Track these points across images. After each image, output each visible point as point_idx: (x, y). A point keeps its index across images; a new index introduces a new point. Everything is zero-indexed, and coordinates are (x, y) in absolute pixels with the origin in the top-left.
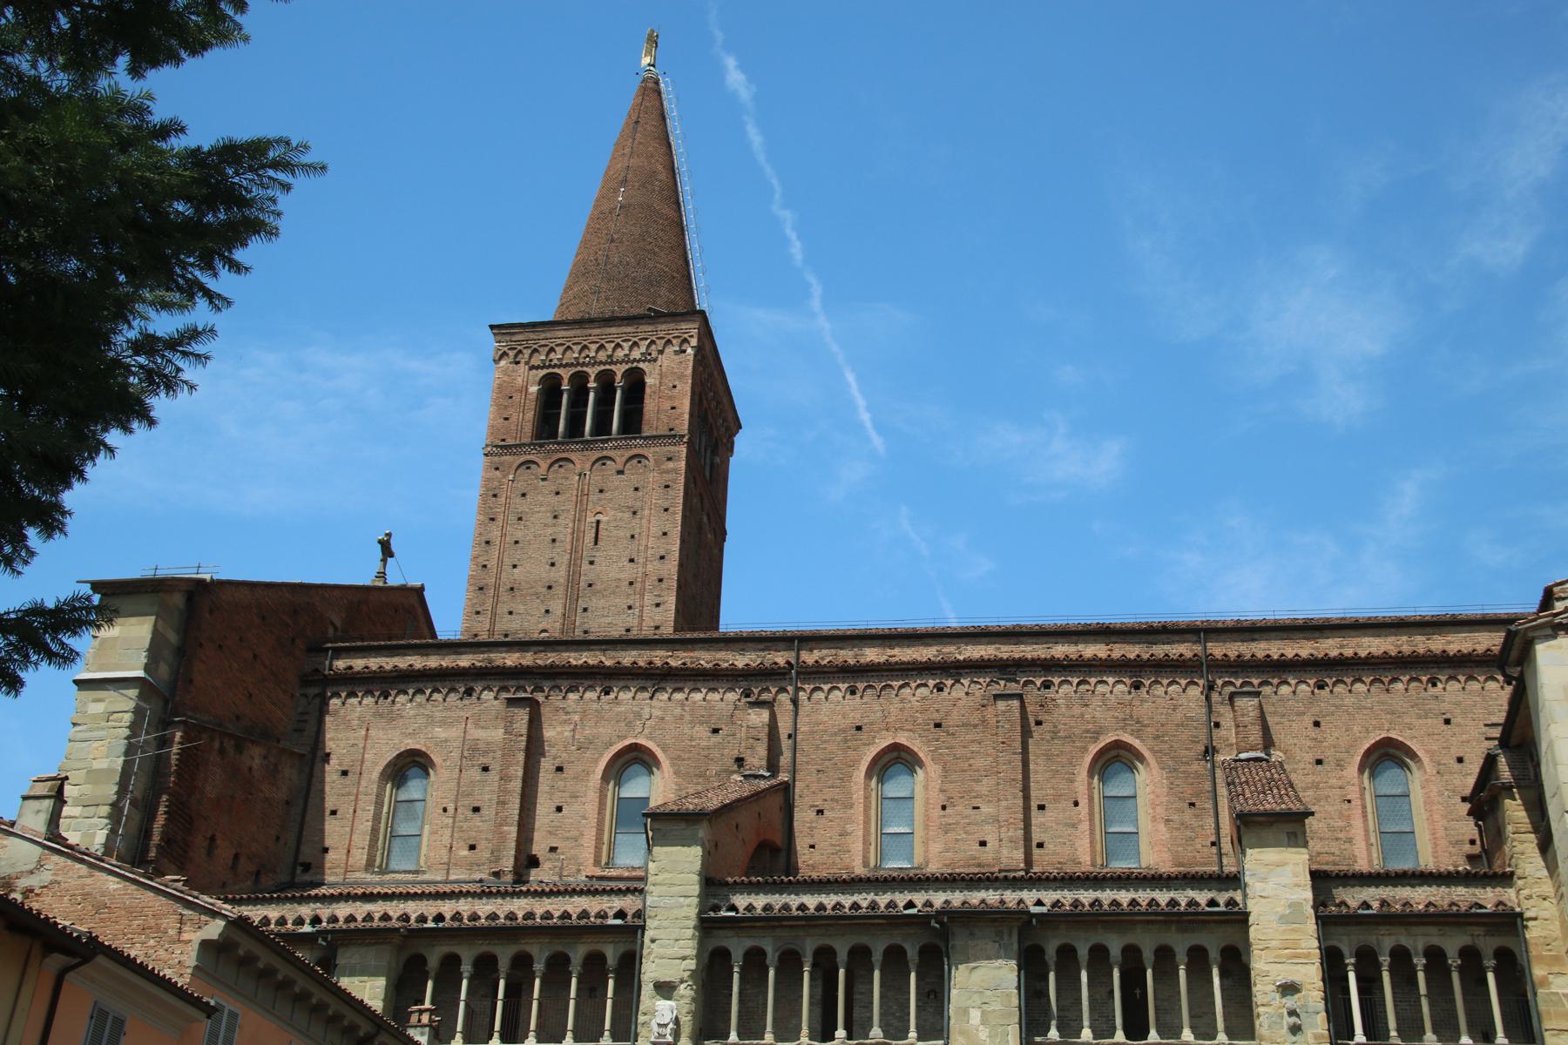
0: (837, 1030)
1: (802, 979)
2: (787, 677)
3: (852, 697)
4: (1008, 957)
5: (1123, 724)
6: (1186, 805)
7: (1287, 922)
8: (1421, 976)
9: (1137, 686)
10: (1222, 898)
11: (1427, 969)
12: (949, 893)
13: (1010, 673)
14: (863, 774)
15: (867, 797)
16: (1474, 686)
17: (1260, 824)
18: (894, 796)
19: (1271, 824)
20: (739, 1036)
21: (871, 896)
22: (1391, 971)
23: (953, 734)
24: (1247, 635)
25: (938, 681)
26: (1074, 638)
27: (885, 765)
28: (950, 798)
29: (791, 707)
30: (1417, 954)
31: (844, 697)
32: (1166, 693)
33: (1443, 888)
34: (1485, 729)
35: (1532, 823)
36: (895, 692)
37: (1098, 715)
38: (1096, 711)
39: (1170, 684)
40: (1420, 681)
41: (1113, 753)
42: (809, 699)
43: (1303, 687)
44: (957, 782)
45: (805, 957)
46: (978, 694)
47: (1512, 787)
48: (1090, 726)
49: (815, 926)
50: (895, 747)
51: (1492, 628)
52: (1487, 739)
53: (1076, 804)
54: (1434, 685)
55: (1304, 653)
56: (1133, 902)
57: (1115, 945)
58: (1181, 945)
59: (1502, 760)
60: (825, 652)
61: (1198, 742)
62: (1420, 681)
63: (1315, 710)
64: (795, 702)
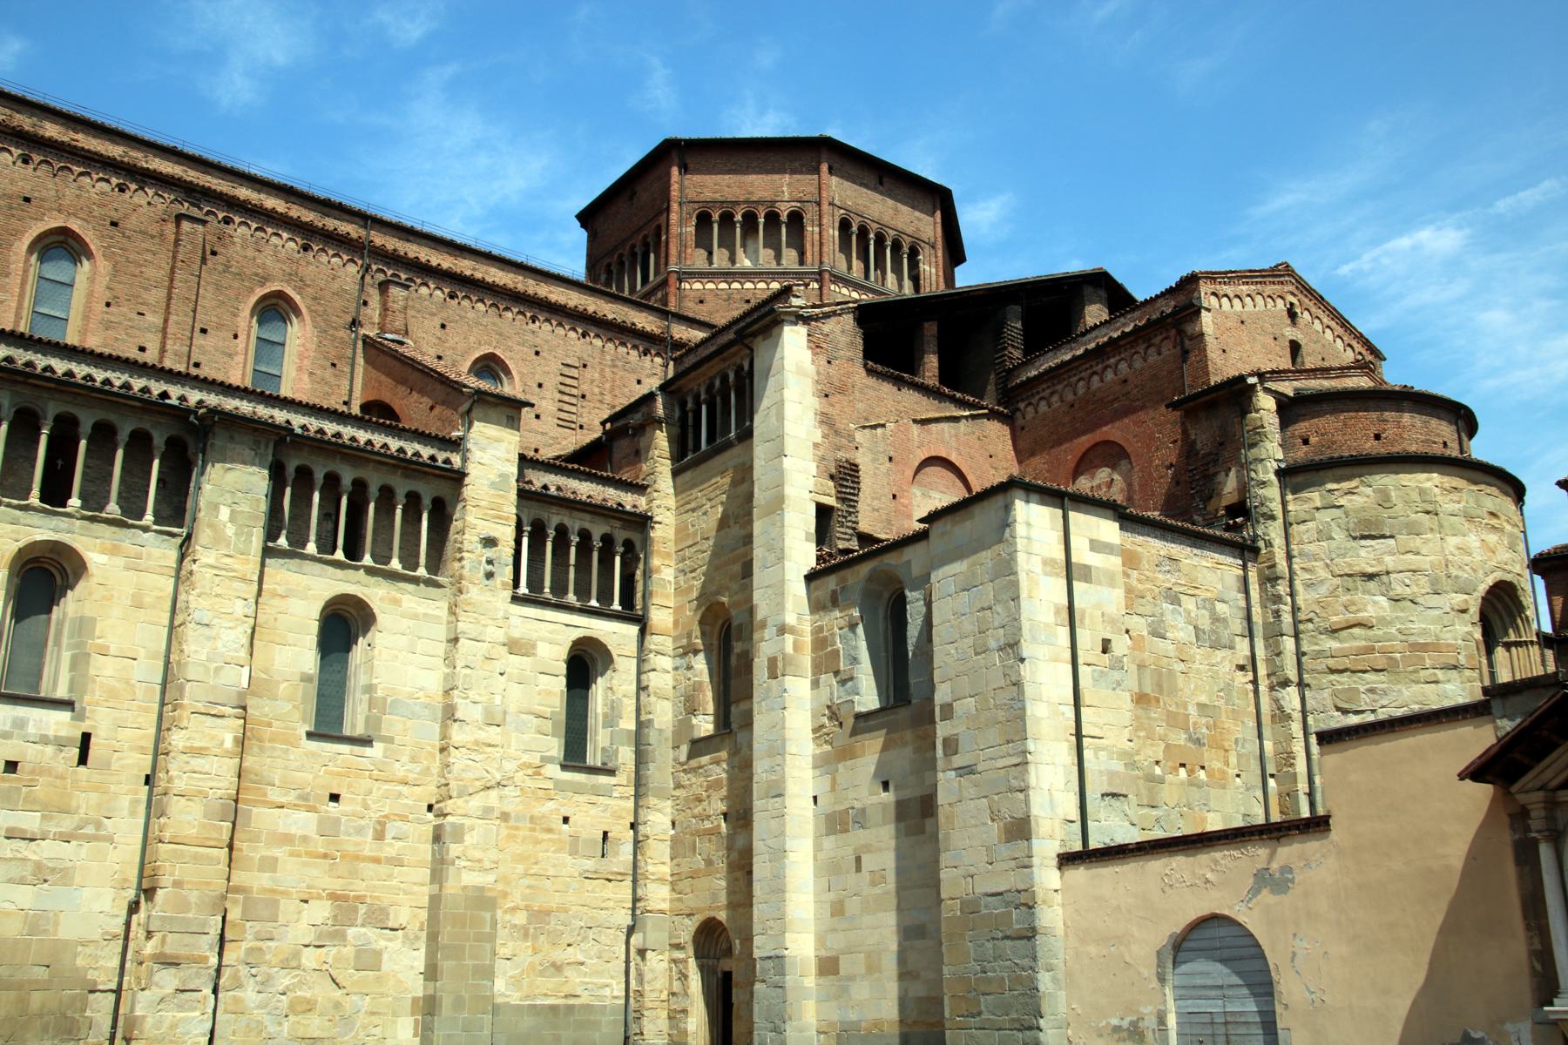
0: (70, 498)
1: (37, 442)
3: (24, 166)
4: (261, 465)
5: (290, 277)
7: (496, 489)
8: (573, 550)
9: (306, 248)
11: (578, 546)
12: (205, 393)
13: (194, 198)
14: (25, 248)
15: (26, 271)
16: (560, 331)
17: (488, 403)
18: (52, 278)
19: (496, 405)
21: (125, 377)
23: (129, 237)
24: (404, 235)
25: (121, 181)
26: (259, 186)
27: (47, 245)
28: (115, 297)
30: (573, 533)
31: (14, 163)
32: (329, 262)
33: (600, 487)
34: (561, 367)
35: (671, 452)
36: (73, 177)
37: (268, 262)
38: (267, 260)
39: (334, 255)
41: (274, 301)
43: (438, 292)
44: (125, 283)
45: (45, 419)
48: (260, 271)
49: (61, 391)
50: (64, 232)
51: (582, 291)
52: (562, 375)
53: (236, 337)
54: (534, 322)
56: (369, 442)
57: (347, 477)
58: (402, 487)
59: (660, 400)
61: (348, 313)
63: (444, 315)
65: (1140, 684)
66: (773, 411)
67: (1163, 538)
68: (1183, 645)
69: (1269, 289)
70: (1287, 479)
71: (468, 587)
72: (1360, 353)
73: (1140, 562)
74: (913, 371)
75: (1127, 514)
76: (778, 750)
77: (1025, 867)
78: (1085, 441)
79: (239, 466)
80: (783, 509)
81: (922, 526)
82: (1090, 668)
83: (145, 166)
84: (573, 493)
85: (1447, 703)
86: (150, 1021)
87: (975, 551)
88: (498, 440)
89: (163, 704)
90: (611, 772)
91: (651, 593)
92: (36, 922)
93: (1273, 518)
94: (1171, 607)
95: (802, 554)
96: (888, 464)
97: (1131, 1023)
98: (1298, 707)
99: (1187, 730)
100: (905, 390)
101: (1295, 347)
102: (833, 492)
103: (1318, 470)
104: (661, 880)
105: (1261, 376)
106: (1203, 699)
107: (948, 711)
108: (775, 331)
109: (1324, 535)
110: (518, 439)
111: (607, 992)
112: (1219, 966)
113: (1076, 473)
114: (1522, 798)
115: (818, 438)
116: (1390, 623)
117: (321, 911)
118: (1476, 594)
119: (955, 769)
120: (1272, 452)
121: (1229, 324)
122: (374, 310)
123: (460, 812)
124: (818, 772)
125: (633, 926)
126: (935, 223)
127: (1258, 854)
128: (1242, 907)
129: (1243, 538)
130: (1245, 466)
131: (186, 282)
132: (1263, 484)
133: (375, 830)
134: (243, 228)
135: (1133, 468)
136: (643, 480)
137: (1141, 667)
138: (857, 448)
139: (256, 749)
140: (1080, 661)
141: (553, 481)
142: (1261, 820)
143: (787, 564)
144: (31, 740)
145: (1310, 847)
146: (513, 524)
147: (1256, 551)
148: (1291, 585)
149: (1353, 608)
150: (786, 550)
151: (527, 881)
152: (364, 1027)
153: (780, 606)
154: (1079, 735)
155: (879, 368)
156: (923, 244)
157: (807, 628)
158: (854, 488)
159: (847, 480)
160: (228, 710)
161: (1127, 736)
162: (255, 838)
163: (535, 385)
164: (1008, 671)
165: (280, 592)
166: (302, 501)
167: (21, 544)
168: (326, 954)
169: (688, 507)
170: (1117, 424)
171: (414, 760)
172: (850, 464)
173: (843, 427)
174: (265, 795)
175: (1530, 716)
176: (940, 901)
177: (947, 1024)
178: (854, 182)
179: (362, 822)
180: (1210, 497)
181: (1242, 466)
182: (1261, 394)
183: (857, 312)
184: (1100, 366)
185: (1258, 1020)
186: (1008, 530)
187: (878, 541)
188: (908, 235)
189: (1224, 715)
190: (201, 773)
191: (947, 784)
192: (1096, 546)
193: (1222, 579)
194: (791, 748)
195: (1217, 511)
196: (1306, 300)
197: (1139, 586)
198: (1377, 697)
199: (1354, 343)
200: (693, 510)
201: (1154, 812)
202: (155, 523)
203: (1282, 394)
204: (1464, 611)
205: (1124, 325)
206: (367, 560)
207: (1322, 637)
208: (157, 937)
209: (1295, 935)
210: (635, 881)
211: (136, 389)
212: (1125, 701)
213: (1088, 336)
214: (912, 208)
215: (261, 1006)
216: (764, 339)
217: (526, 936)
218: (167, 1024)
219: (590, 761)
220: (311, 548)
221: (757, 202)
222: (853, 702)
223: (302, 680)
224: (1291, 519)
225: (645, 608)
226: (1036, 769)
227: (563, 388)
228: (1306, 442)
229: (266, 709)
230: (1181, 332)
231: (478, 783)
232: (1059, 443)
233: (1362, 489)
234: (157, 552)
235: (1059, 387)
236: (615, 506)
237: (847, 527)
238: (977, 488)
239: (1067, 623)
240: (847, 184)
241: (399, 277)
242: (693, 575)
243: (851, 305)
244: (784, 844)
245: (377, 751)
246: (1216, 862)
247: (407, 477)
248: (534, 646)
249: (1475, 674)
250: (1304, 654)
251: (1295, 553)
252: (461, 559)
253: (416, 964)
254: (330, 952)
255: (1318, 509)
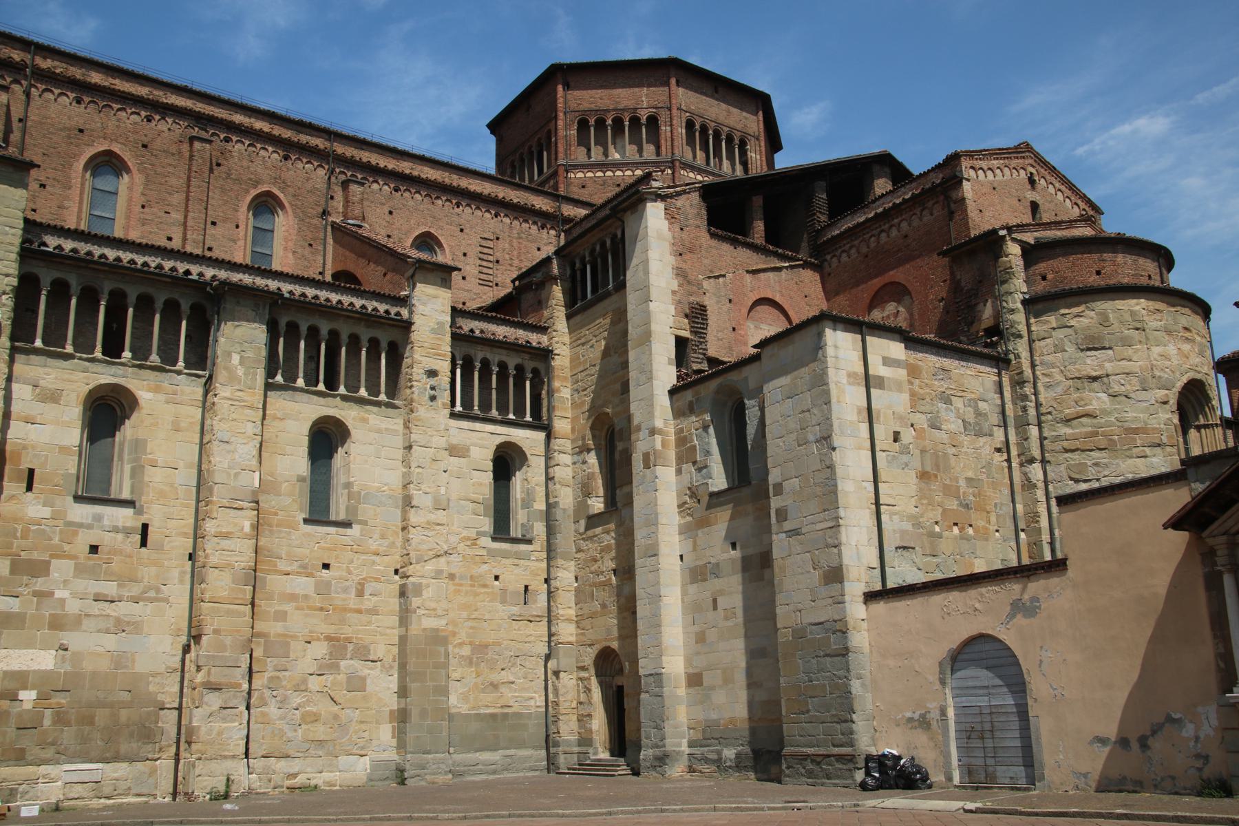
0: (123, 351)
1: (98, 311)
2: (22, 72)
3: (78, 105)
5: (275, 180)
6: (307, 245)
8: (494, 377)
9: (286, 158)
10: (393, 310)
11: (498, 374)
12: (217, 270)
13: (202, 124)
14: (81, 166)
15: (83, 185)
16: (478, 213)
18: (102, 188)
19: (433, 270)
20: (44, 342)
21: (158, 260)
22: (479, 372)
23: (155, 156)
25: (148, 114)
26: (250, 113)
29: (24, 98)
30: (494, 365)
31: (71, 104)
34: (480, 240)
36: (113, 112)
38: (257, 167)
39: (307, 163)
40: (452, 203)
41: (264, 199)
42: (40, 96)
43: (386, 187)
45: (103, 294)
46: (178, 132)
47: (557, 279)
48: (253, 177)
50: (109, 153)
52: (481, 246)
53: (237, 227)
54: (458, 207)
55: (390, 167)
56: (339, 302)
58: (365, 335)
59: (555, 262)
60: (57, 63)
62: (452, 203)
64: (28, 95)
65: (922, 464)
66: (641, 267)
67: (937, 354)
68: (953, 435)
69: (1014, 163)
70: (1031, 307)
71: (417, 408)
72: (1084, 210)
73: (921, 373)
74: (745, 235)
75: (910, 337)
76: (653, 522)
77: (839, 603)
78: (877, 283)
79: (245, 323)
80: (650, 342)
81: (756, 350)
82: (884, 454)
83: (165, 101)
84: (493, 334)
85: (1154, 472)
86: (203, 729)
87: (796, 369)
88: (436, 297)
89: (198, 501)
90: (529, 542)
91: (554, 407)
92: (119, 660)
93: (1020, 336)
94: (945, 406)
95: (665, 374)
96: (728, 305)
97: (921, 715)
98: (1042, 478)
99: (958, 498)
100: (739, 248)
101: (1034, 207)
102: (688, 327)
103: (1054, 299)
104: (569, 620)
105: (1009, 229)
106: (970, 474)
107: (779, 488)
108: (640, 207)
109: (1059, 349)
110: (450, 295)
111: (532, 703)
112: (985, 672)
113: (871, 307)
114: (1210, 541)
115: (676, 288)
116: (1110, 413)
117: (320, 649)
118: (1174, 389)
119: (786, 532)
120: (1019, 286)
121: (984, 191)
122: (338, 202)
123: (418, 574)
124: (683, 537)
125: (550, 654)
126: (758, 121)
127: (1013, 588)
128: (1003, 628)
129: (998, 352)
130: (998, 298)
131: (199, 187)
132: (1012, 311)
133: (357, 589)
134: (239, 144)
135: (914, 302)
136: (545, 322)
137: (923, 451)
138: (705, 293)
139: (267, 532)
140: (877, 448)
141: (477, 326)
142: (1015, 563)
143: (655, 382)
144: (106, 529)
145: (1054, 582)
146: (449, 359)
147: (1008, 362)
148: (1035, 387)
149: (1082, 403)
150: (654, 372)
151: (470, 624)
152: (356, 732)
153: (651, 414)
154: (877, 504)
155: (720, 232)
156: (749, 137)
157: (671, 430)
158: (703, 324)
159: (698, 318)
160: (245, 504)
161: (914, 504)
162: (270, 597)
163: (461, 254)
164: (823, 458)
165: (279, 416)
166: (292, 348)
167: (91, 387)
168: (326, 680)
169: (579, 342)
170: (901, 269)
171: (383, 537)
172: (700, 306)
173: (693, 277)
174: (276, 566)
175: (1216, 480)
176: (776, 630)
177: (784, 720)
178: (696, 91)
179: (347, 584)
180: (972, 323)
181: (996, 298)
182: (1009, 243)
183: (701, 191)
184: (887, 226)
185: (1015, 710)
186: (820, 352)
187: (723, 363)
188: (738, 131)
189: (986, 486)
190: (228, 551)
191: (780, 543)
192: (887, 362)
193: (983, 384)
194: (662, 520)
195: (978, 332)
196: (1042, 170)
197: (920, 390)
198: (1100, 469)
199: (1079, 202)
200: (583, 344)
201: (935, 560)
202: (186, 368)
203: (1025, 242)
204: (1165, 403)
205: (905, 193)
206: (342, 390)
207: (1059, 425)
208: (204, 670)
209: (1041, 647)
210: (549, 622)
211: (167, 269)
212: (912, 477)
213: (877, 203)
214: (740, 109)
215: (281, 718)
216: (632, 213)
217: (471, 664)
218: (215, 732)
219: (513, 534)
220: (300, 382)
221: (623, 110)
222: (708, 484)
223: (298, 481)
224: (1034, 337)
225: (550, 419)
226: (846, 530)
227: (481, 256)
228: (1044, 278)
229: (273, 503)
230: (948, 198)
231: (431, 553)
232: (857, 284)
233: (1087, 312)
234: (188, 389)
235: (856, 243)
236: (524, 343)
237: (699, 353)
238: (796, 321)
239: (867, 420)
240: (690, 93)
241: (356, 177)
242: (585, 393)
243: (697, 185)
244: (659, 590)
245: (355, 530)
246: (982, 595)
247: (368, 327)
248: (468, 450)
249: (1174, 450)
250: (1045, 438)
251: (1037, 363)
252: (411, 387)
253: (391, 686)
254: (329, 679)
255: (1054, 329)
